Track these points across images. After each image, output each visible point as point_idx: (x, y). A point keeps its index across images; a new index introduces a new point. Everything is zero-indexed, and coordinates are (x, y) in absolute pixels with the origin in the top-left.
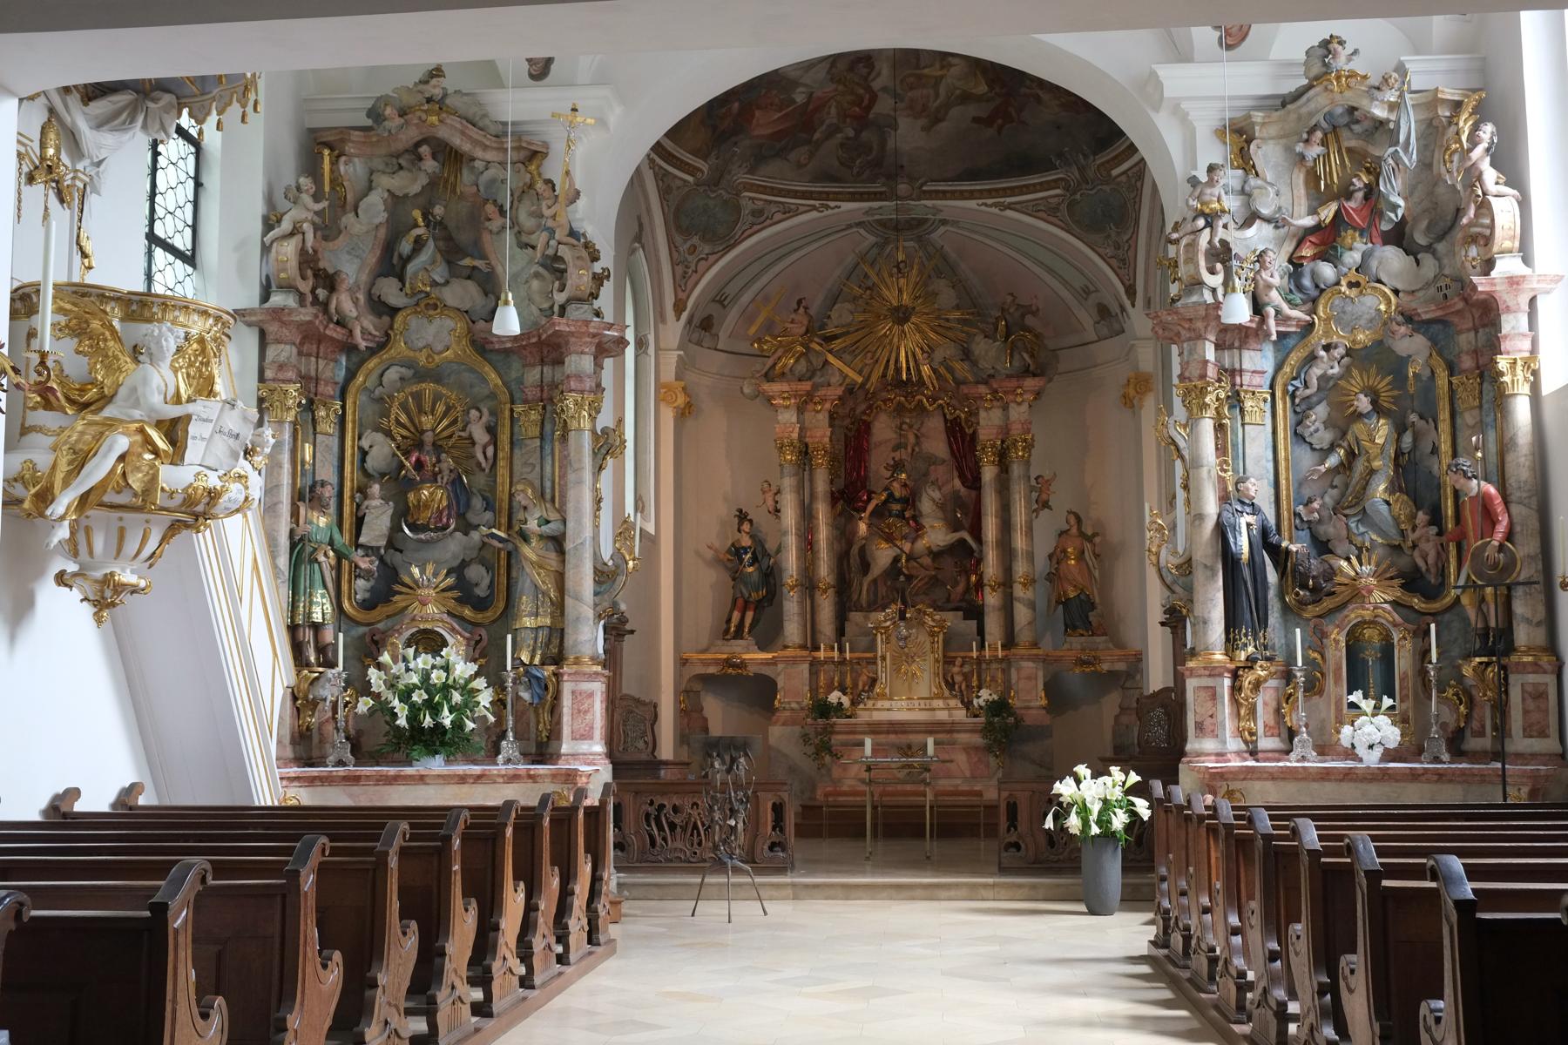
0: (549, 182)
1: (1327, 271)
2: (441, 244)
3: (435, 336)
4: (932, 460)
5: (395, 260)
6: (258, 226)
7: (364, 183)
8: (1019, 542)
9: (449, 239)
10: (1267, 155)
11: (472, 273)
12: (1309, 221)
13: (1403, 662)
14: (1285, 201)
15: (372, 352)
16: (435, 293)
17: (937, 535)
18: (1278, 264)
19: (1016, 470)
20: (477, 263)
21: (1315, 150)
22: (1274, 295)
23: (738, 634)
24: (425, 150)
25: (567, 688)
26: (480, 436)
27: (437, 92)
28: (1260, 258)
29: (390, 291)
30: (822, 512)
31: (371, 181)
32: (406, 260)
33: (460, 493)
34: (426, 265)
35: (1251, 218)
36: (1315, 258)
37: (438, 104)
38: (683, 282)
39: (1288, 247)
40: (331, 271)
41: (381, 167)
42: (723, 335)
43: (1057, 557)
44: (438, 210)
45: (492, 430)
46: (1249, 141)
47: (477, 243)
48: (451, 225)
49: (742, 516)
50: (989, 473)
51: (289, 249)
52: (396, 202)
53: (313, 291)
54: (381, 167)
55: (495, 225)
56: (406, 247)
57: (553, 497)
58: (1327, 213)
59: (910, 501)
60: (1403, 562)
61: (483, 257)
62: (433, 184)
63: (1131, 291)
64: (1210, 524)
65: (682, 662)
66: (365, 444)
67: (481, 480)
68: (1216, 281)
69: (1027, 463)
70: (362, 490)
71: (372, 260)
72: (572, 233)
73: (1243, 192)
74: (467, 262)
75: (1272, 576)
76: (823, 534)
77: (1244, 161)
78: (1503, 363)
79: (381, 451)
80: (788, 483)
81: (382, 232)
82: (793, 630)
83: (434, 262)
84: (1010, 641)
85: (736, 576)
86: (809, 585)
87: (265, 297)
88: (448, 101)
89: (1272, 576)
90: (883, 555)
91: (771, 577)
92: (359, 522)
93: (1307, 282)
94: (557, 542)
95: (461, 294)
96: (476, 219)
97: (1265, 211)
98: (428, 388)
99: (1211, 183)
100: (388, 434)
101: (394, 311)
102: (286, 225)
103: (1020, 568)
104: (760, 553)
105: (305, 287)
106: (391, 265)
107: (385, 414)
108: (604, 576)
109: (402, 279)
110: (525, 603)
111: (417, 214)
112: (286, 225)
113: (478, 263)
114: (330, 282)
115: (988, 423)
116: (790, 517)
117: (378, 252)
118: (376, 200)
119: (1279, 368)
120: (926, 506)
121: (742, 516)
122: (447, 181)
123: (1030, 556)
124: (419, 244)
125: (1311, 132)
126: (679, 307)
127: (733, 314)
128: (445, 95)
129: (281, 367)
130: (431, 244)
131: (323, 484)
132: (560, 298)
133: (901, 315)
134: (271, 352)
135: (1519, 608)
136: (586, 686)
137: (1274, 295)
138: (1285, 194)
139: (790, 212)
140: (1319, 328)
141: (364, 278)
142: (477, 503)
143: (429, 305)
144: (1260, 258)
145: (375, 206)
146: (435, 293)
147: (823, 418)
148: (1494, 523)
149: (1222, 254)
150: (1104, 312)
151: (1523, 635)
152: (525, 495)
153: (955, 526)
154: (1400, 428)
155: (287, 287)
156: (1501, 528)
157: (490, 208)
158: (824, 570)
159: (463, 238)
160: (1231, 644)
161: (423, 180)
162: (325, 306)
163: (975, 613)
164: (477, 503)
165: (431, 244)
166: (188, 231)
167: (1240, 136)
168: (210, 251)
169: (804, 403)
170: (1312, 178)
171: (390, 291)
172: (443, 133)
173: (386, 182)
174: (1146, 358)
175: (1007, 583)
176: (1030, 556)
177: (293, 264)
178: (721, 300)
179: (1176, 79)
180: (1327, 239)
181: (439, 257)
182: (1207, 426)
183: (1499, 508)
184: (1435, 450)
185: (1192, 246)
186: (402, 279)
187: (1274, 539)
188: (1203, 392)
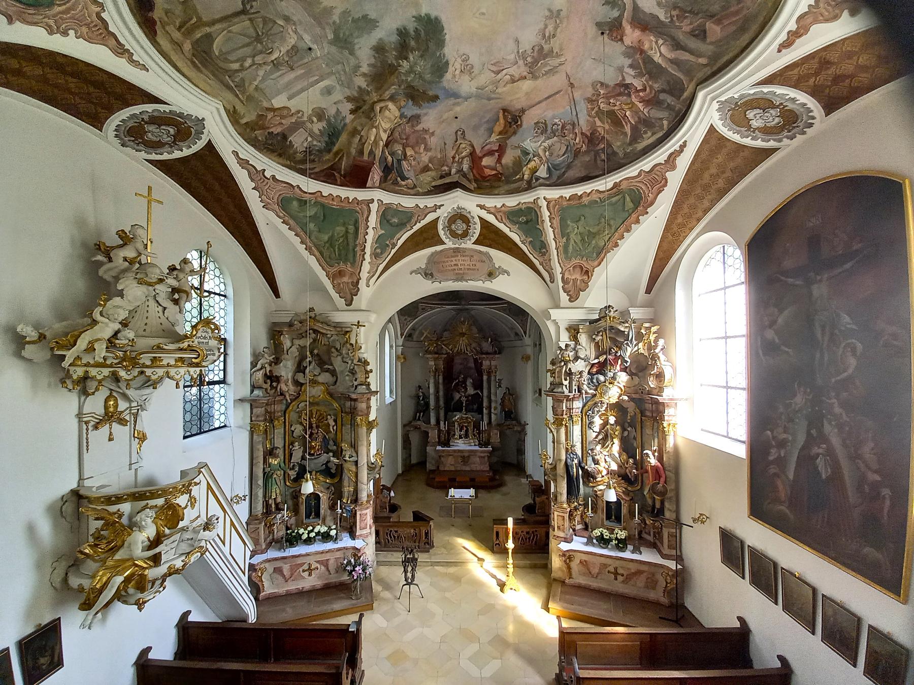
0: (352, 344)
1: (602, 378)
3: (317, 392)
4: (470, 368)
6: (248, 366)
8: (493, 398)
9: (320, 359)
10: (583, 338)
11: (328, 370)
12: (596, 361)
13: (624, 510)
14: (588, 353)
15: (292, 401)
16: (315, 378)
17: (471, 391)
18: (586, 375)
19: (493, 378)
20: (330, 367)
21: (599, 338)
22: (585, 387)
23: (419, 419)
25: (358, 513)
26: (332, 423)
27: (313, 315)
28: (581, 373)
29: (300, 377)
30: (441, 387)
33: (325, 441)
34: (312, 369)
35: (577, 358)
36: (597, 373)
37: (314, 319)
38: (402, 329)
39: (588, 368)
42: (415, 337)
43: (503, 399)
44: (316, 352)
45: (335, 421)
46: (578, 332)
47: (330, 359)
48: (321, 354)
49: (420, 387)
50: (485, 377)
51: (260, 375)
52: (302, 349)
55: (334, 355)
57: (354, 446)
58: (602, 359)
59: (464, 382)
60: (623, 471)
61: (332, 365)
62: (315, 340)
63: (525, 333)
64: (563, 462)
65: (404, 426)
66: (293, 429)
67: (332, 435)
68: (566, 383)
69: (495, 376)
70: (292, 444)
72: (360, 360)
73: (574, 349)
75: (580, 472)
76: (441, 393)
77: (575, 338)
78: (665, 425)
79: (298, 430)
80: (432, 381)
82: (433, 421)
83: (314, 368)
84: (490, 423)
85: (418, 403)
86: (437, 407)
87: (252, 392)
89: (580, 472)
90: (457, 396)
91: (427, 404)
92: (291, 455)
93: (595, 381)
94: (356, 463)
95: (325, 377)
96: (329, 352)
97: (582, 357)
98: (314, 409)
99: (566, 350)
100: (301, 423)
101: (302, 385)
102: (259, 366)
103: (493, 405)
104: (426, 397)
105: (268, 386)
106: (300, 368)
107: (300, 417)
108: (371, 467)
110: (346, 483)
112: (259, 366)
113: (330, 367)
114: (277, 379)
115: (486, 364)
116: (432, 390)
118: (294, 349)
119: (584, 406)
120: (468, 383)
121: (420, 387)
123: (496, 402)
125: (599, 332)
126: (402, 335)
127: (417, 332)
129: (258, 416)
131: (277, 448)
132: (356, 383)
133: (463, 334)
134: (255, 410)
135: (667, 505)
136: (364, 512)
137: (585, 387)
138: (587, 349)
139: (432, 309)
140: (598, 395)
141: (290, 375)
142: (331, 443)
143: (314, 382)
144: (581, 373)
145: (294, 351)
146: (315, 378)
147: (441, 362)
148: (660, 477)
149: (570, 374)
150: (517, 334)
151: (668, 514)
152: (345, 446)
153: (475, 389)
154: (624, 429)
155: (260, 388)
156: (662, 480)
157: (333, 350)
158: (442, 403)
159: (325, 358)
160: (569, 501)
163: (481, 413)
164: (331, 443)
166: (222, 372)
167: (574, 331)
168: (230, 378)
169: (435, 359)
170: (597, 345)
171: (300, 377)
173: (297, 342)
174: (529, 351)
175: (489, 408)
176: (496, 402)
177: (261, 381)
178: (413, 329)
179: (555, 314)
180: (602, 368)
182: (563, 430)
183: (662, 472)
184: (635, 438)
185: (560, 371)
187: (583, 465)
188: (562, 420)
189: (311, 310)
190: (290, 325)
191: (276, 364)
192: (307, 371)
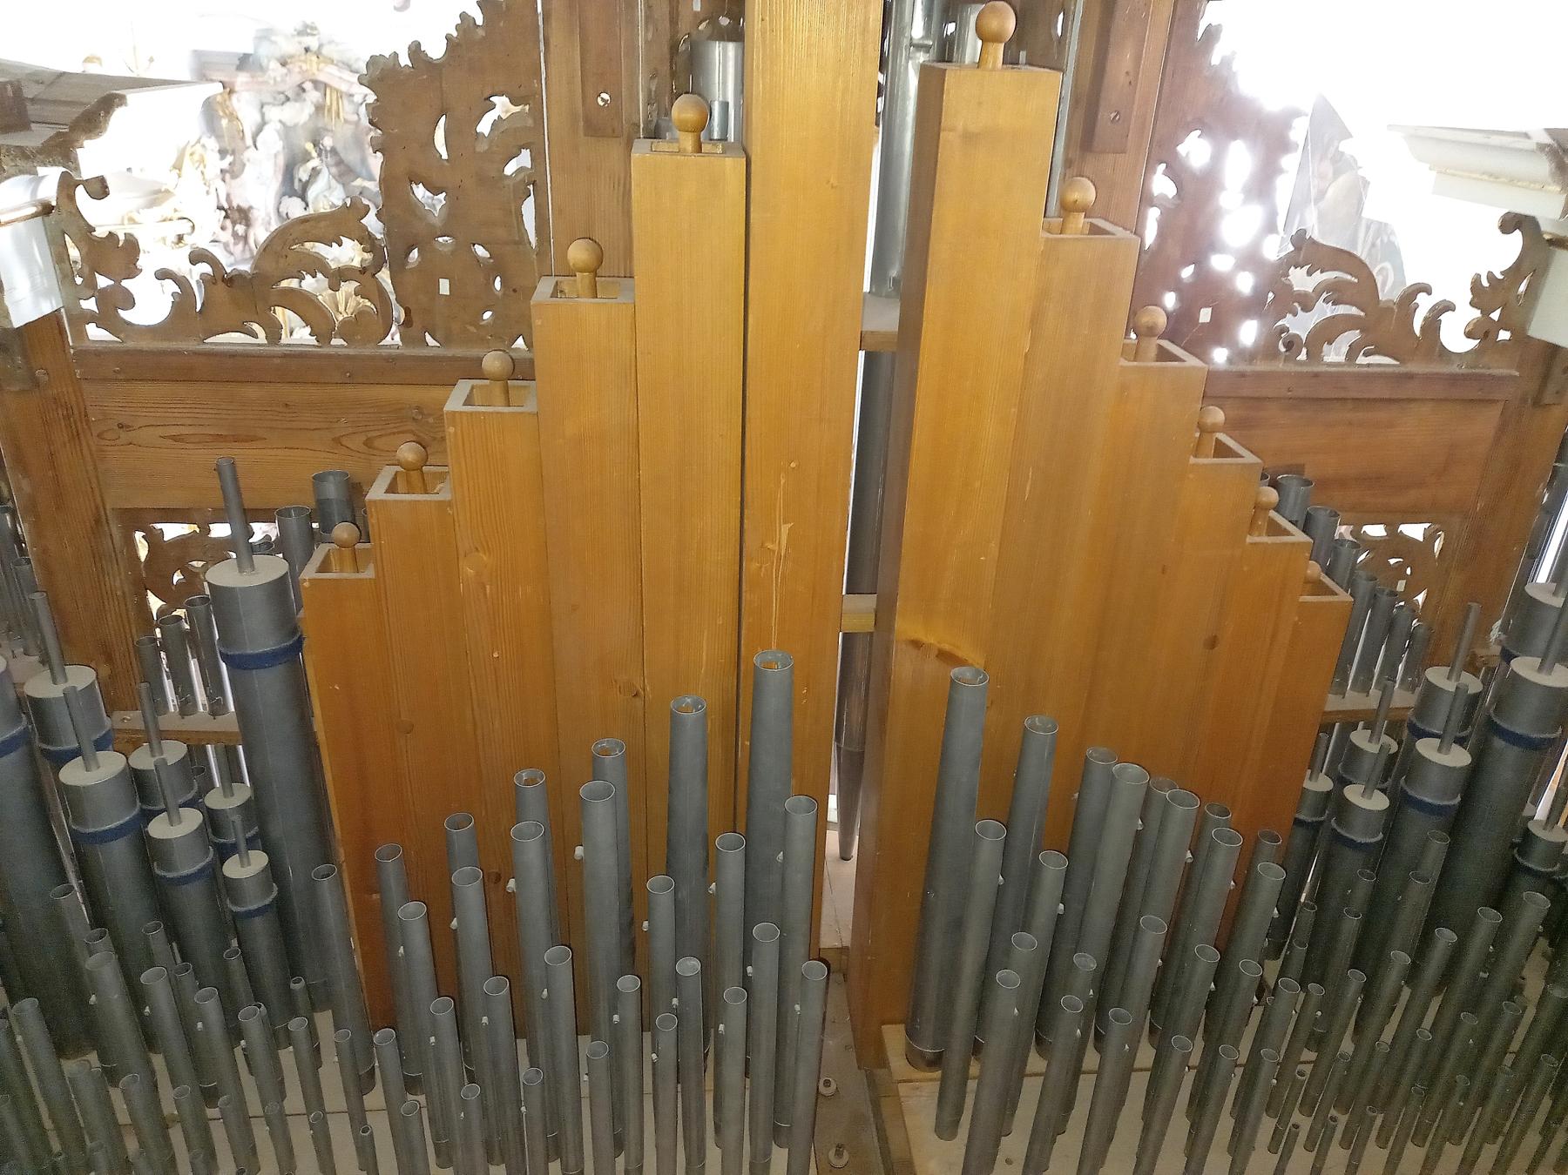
2: (334, 170)
5: (297, 185)
7: (258, 118)
9: (340, 163)
24: (308, 86)
31: (263, 115)
32: (305, 186)
40: (244, 205)
41: (270, 100)
44: (328, 142)
48: (339, 148)
52: (287, 131)
53: (235, 234)
54: (270, 100)
56: (303, 174)
62: (319, 108)
71: (275, 184)
74: (359, 182)
81: (281, 161)
88: (325, 51)
109: (303, 198)
111: (309, 146)
117: (280, 178)
122: (330, 110)
124: (315, 173)
128: (321, 46)
130: (325, 172)
145: (272, 142)
161: (309, 109)
162: (245, 238)
165: (325, 172)
172: (321, 77)
181: (333, 182)
186: (303, 198)
189: (307, 30)
190: (288, 99)
191: (234, 176)
192: (312, 193)
